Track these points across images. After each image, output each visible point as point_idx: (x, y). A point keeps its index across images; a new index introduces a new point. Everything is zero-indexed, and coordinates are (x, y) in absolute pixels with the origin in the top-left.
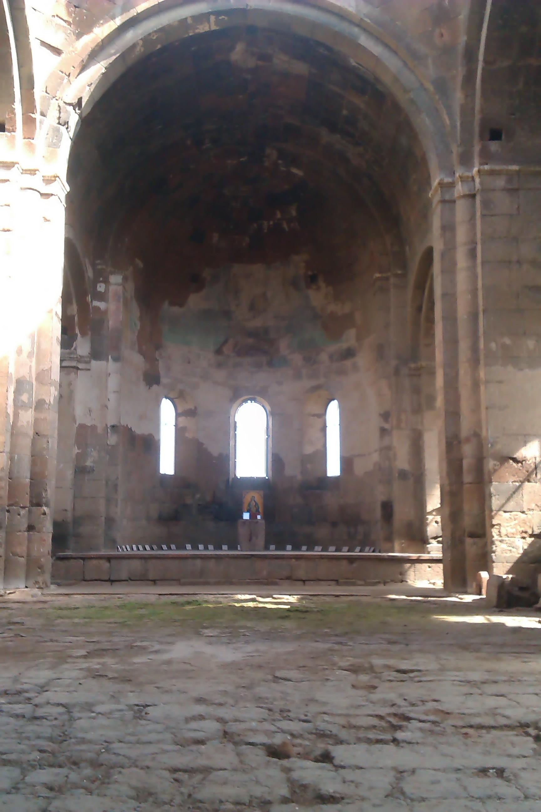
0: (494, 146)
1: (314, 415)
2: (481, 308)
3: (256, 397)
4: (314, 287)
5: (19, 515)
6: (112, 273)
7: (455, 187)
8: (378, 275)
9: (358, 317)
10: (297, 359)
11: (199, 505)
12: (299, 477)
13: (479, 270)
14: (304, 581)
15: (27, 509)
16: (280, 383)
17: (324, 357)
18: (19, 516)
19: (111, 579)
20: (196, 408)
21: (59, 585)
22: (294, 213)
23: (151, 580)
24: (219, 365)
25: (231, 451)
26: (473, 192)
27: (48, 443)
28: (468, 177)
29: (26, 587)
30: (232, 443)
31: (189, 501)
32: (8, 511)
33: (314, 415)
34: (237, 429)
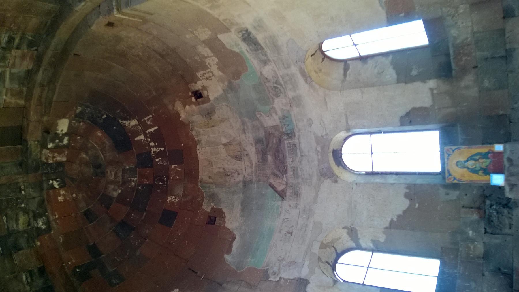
1: (345, 75)
3: (331, 149)
4: (205, 93)
8: (115, 11)
9: (204, 34)
10: (279, 103)
11: (486, 232)
12: (432, 83)
16: (310, 123)
17: (267, 71)
20: (344, 228)
22: (134, 122)
24: (296, 195)
25: (402, 180)
30: (391, 180)
31: (480, 249)
33: (345, 75)
34: (375, 170)
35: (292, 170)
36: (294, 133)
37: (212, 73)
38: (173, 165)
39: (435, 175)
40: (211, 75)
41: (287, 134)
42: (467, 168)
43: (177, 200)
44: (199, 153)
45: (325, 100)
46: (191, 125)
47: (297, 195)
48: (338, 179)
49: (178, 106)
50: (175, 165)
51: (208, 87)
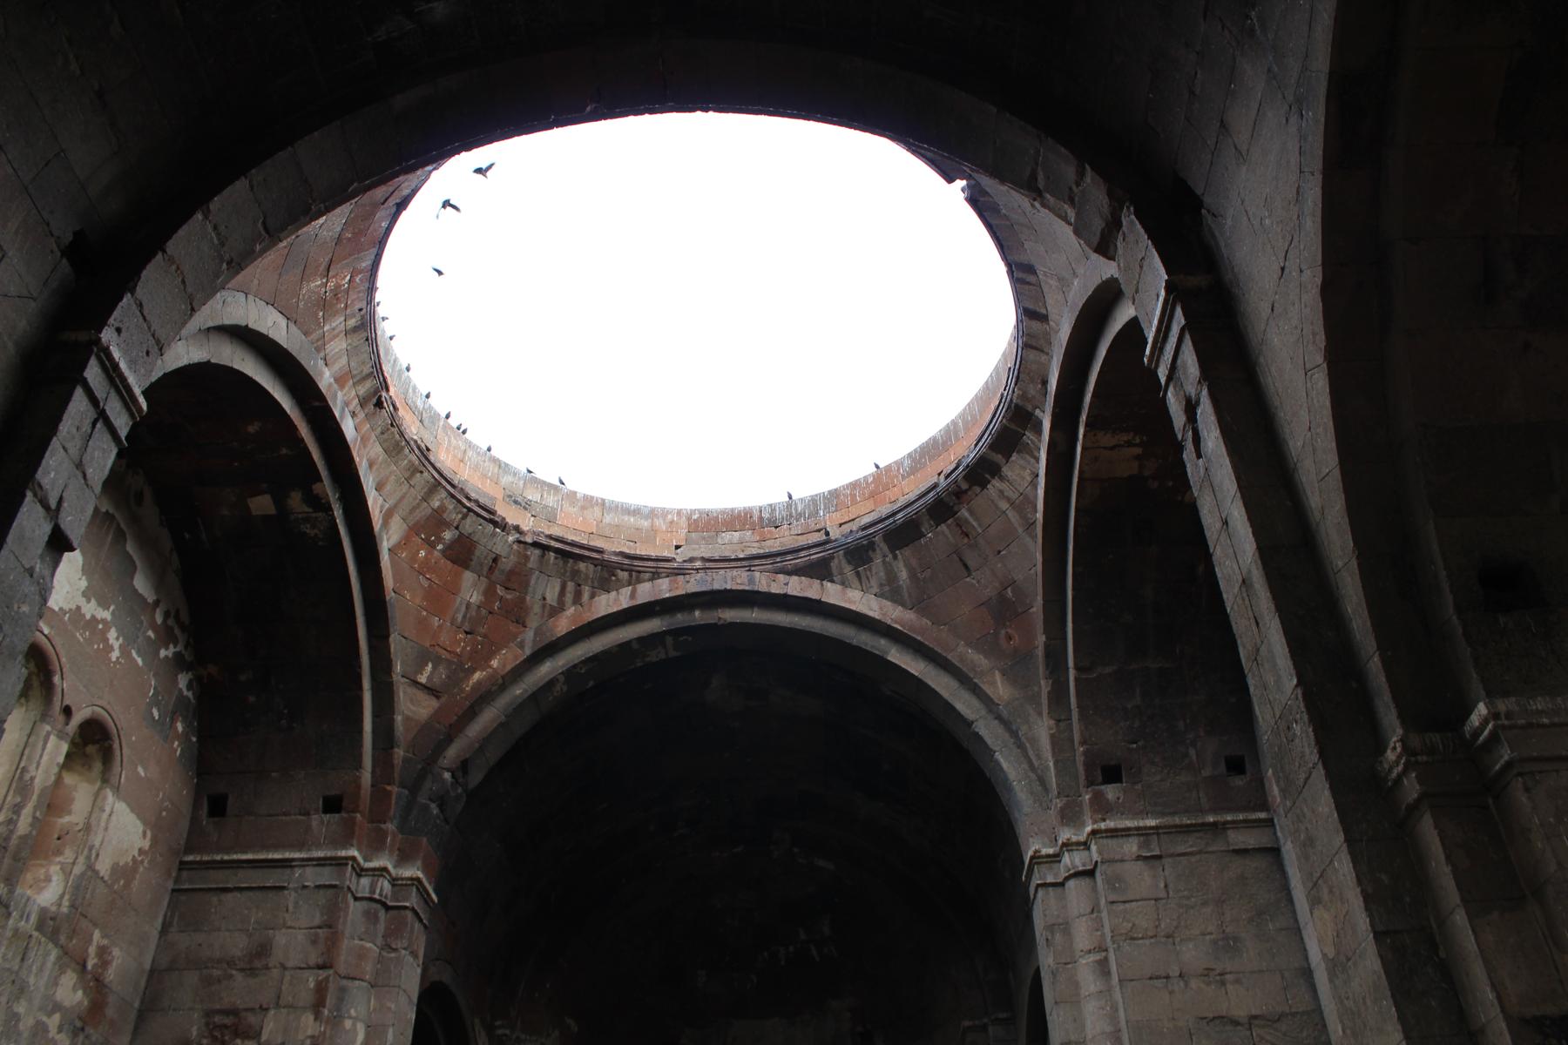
0: (1111, 792)
7: (1060, 861)
8: (967, 1023)
13: (1118, 995)
26: (1088, 868)
28: (1078, 844)
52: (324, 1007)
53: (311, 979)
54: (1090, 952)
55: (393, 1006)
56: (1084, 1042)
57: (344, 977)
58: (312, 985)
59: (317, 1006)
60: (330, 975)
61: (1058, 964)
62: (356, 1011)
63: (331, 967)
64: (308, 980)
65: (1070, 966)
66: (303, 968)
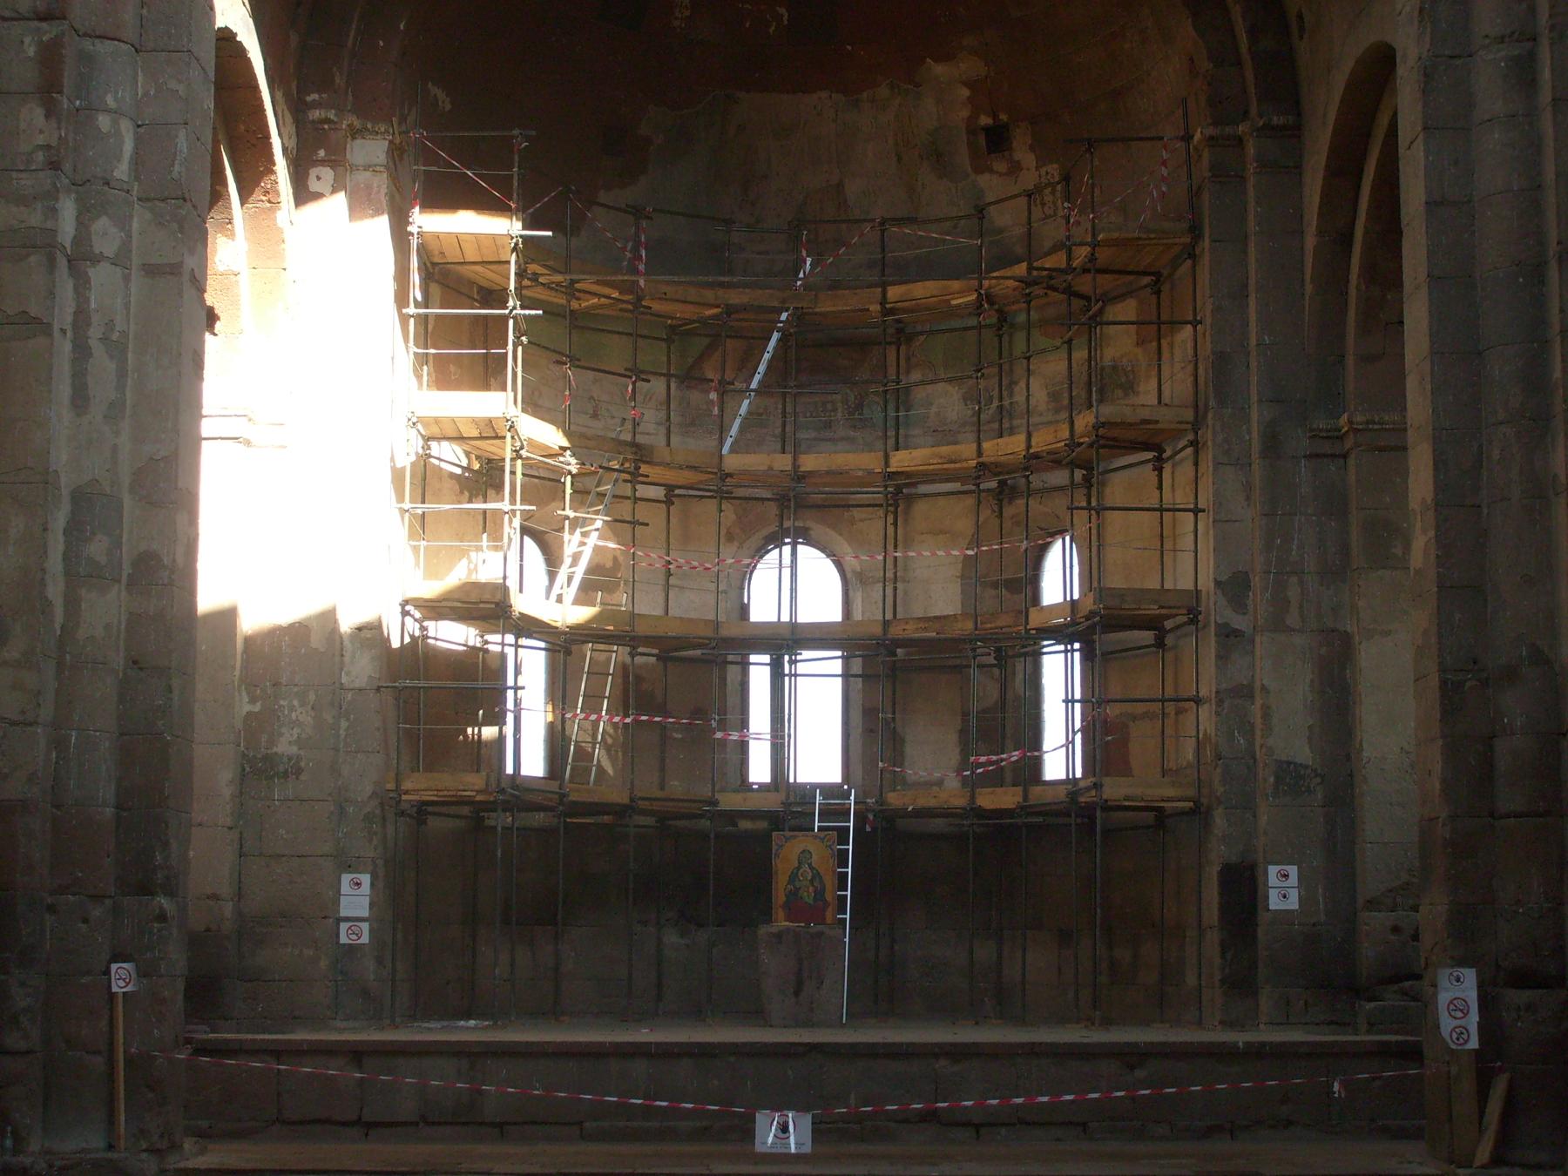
2: (1553, 249)
3: (809, 524)
4: (1001, 166)
5: (85, 921)
6: (355, 133)
8: (1210, 131)
14: (978, 1127)
15: (108, 902)
18: (85, 926)
19: (367, 1117)
20: (615, 559)
21: (201, 1134)
23: (492, 1125)
27: (171, 692)
29: (111, 1147)
32: (51, 909)
35: (761, 411)
36: (863, 427)
37: (1051, 216)
38: (787, 11)
39: (741, 770)
40: (1049, 212)
41: (860, 406)
42: (798, 868)
43: (676, 23)
44: (820, 98)
45: (942, 532)
46: (910, 87)
47: (693, 424)
48: (736, 543)
49: (969, 66)
50: (786, 17)
51: (1016, 182)
52: (60, 92)
53: (27, 40)
54: (1502, 39)
55: (181, 89)
56: (1469, 201)
57: (86, 35)
58: (31, 51)
59: (48, 90)
60: (63, 34)
61: (1436, 56)
62: (116, 100)
63: (65, 18)
64: (22, 42)
65: (1458, 62)
66: (13, 19)
